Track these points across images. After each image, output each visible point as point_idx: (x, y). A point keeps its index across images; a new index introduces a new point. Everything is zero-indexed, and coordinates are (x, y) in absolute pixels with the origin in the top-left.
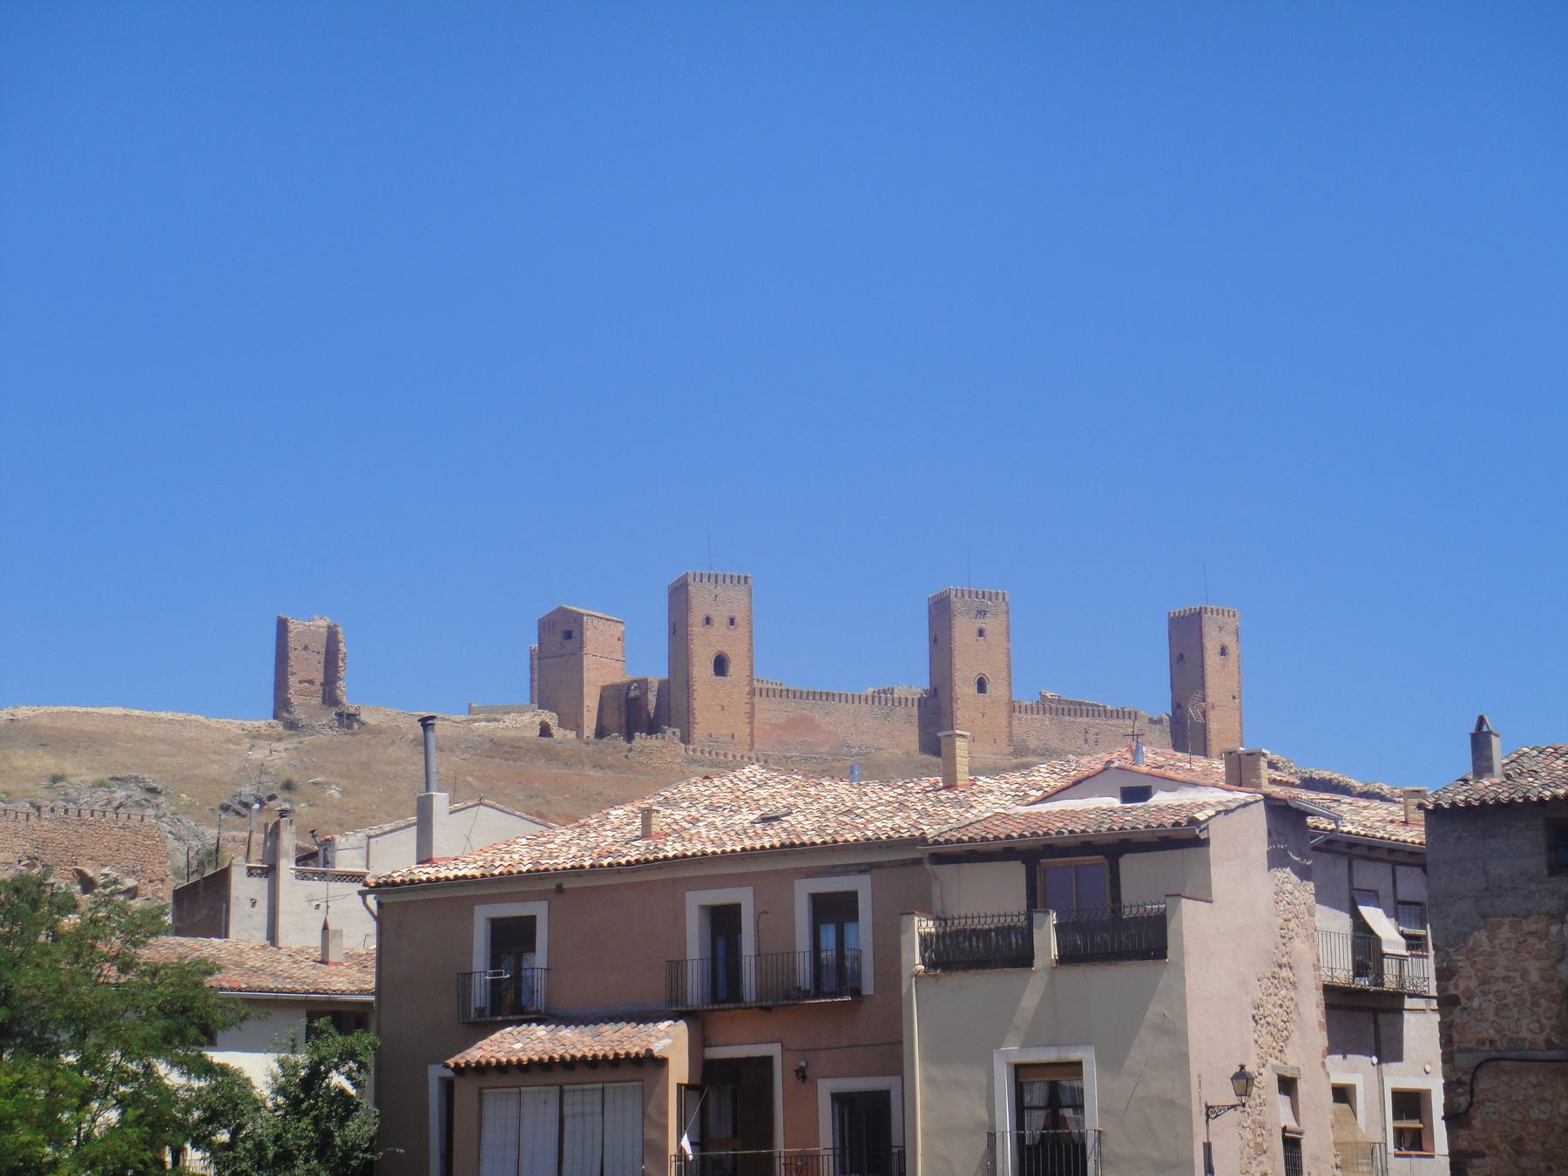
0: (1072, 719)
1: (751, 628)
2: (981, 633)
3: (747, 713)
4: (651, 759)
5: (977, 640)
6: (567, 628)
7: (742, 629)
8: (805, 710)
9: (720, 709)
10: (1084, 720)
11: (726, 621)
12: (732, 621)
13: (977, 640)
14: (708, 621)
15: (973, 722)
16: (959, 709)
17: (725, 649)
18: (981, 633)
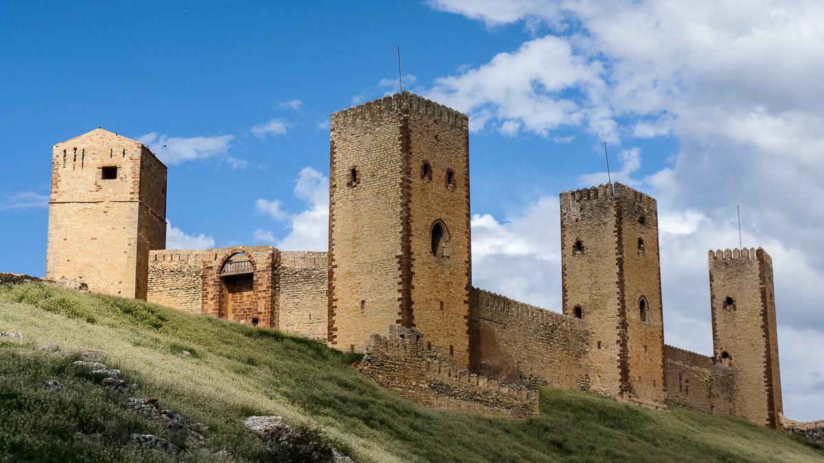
0: (672, 362)
1: (468, 191)
2: (640, 241)
3: (465, 317)
4: (393, 379)
5: (638, 254)
6: (109, 162)
7: (460, 192)
8: (487, 320)
9: (439, 306)
10: (678, 363)
11: (444, 174)
12: (450, 174)
13: (638, 254)
14: (426, 169)
15: (639, 357)
16: (628, 338)
17: (444, 216)
18: (640, 241)
